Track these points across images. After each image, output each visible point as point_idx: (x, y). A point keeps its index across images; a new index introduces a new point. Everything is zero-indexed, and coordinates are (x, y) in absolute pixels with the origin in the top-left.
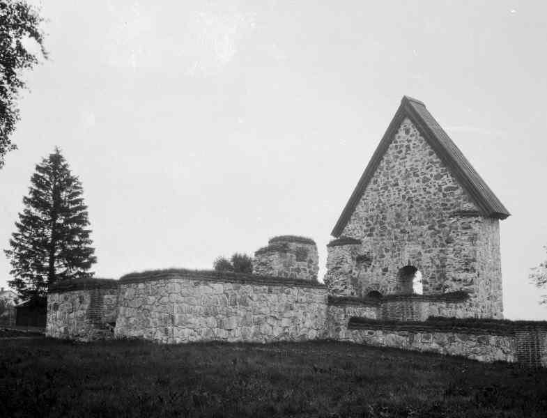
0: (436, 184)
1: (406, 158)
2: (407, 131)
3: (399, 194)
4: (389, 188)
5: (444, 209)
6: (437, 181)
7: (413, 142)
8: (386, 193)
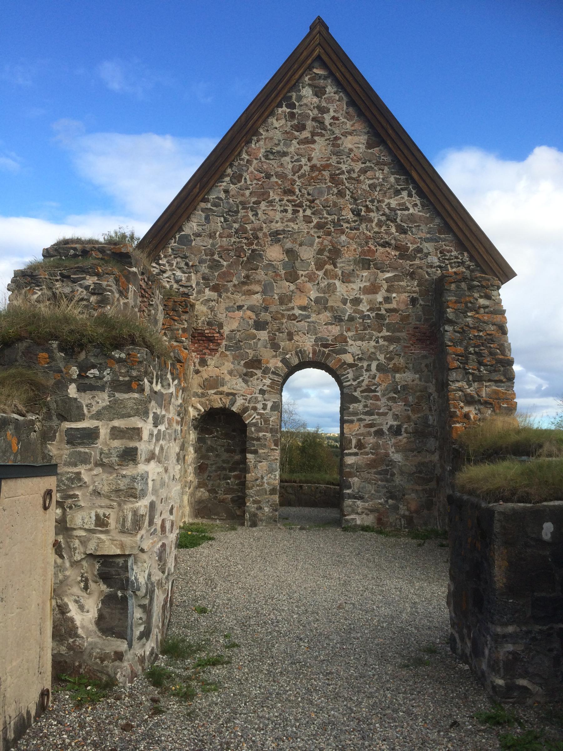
0: (383, 205)
1: (314, 142)
2: (319, 92)
3: (295, 212)
4: (273, 195)
5: (401, 257)
6: (387, 201)
7: (332, 113)
8: (263, 205)
